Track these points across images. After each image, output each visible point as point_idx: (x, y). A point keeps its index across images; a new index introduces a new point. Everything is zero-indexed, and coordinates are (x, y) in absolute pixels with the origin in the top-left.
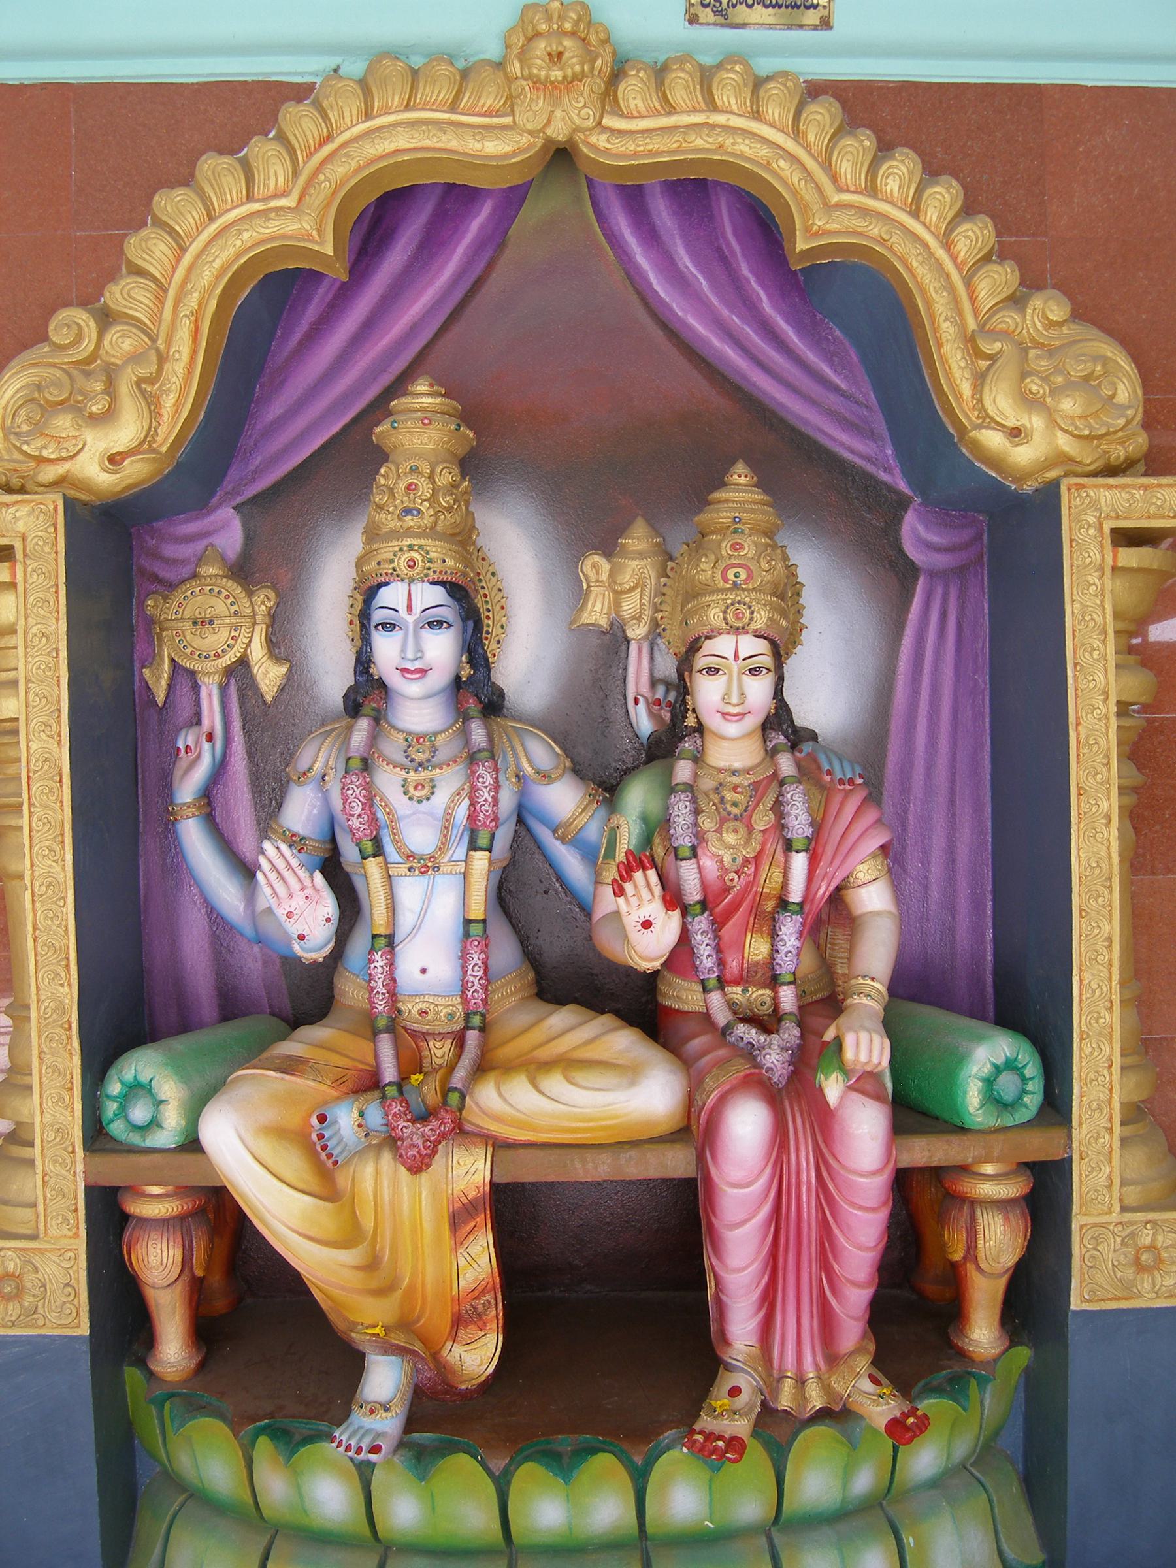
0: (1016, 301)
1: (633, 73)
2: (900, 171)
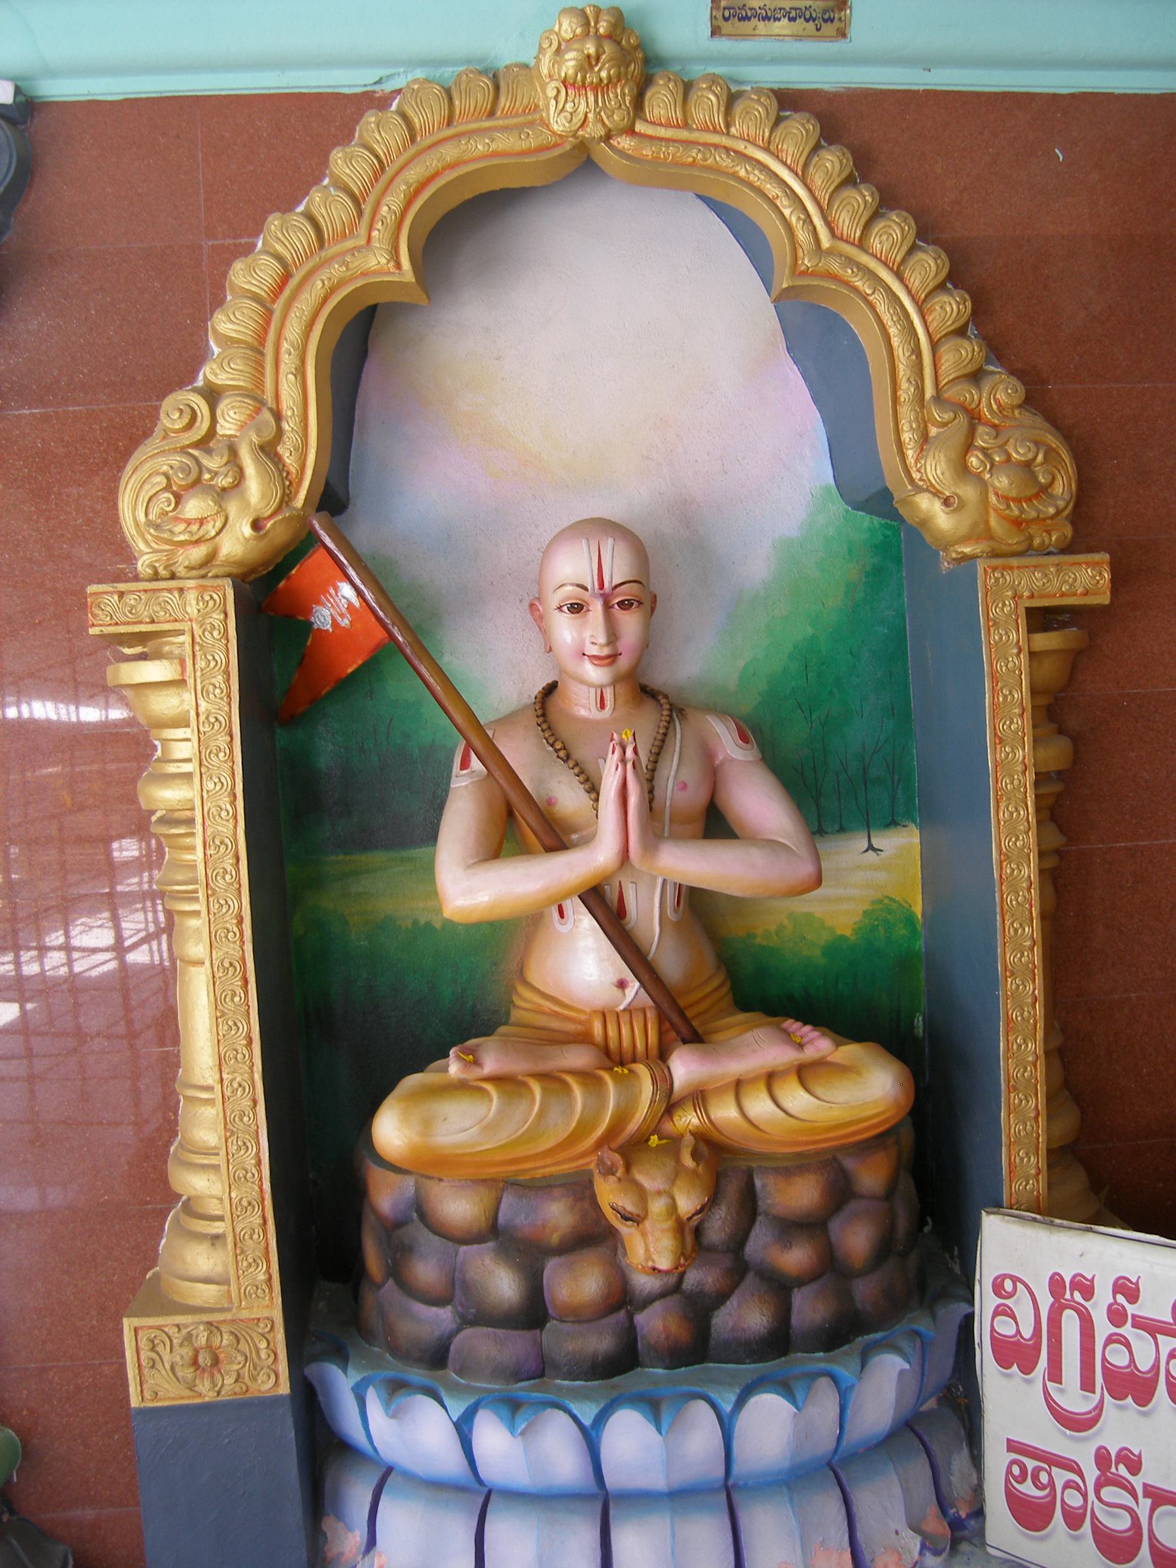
0: (975, 377)
1: (661, 82)
2: (893, 233)
